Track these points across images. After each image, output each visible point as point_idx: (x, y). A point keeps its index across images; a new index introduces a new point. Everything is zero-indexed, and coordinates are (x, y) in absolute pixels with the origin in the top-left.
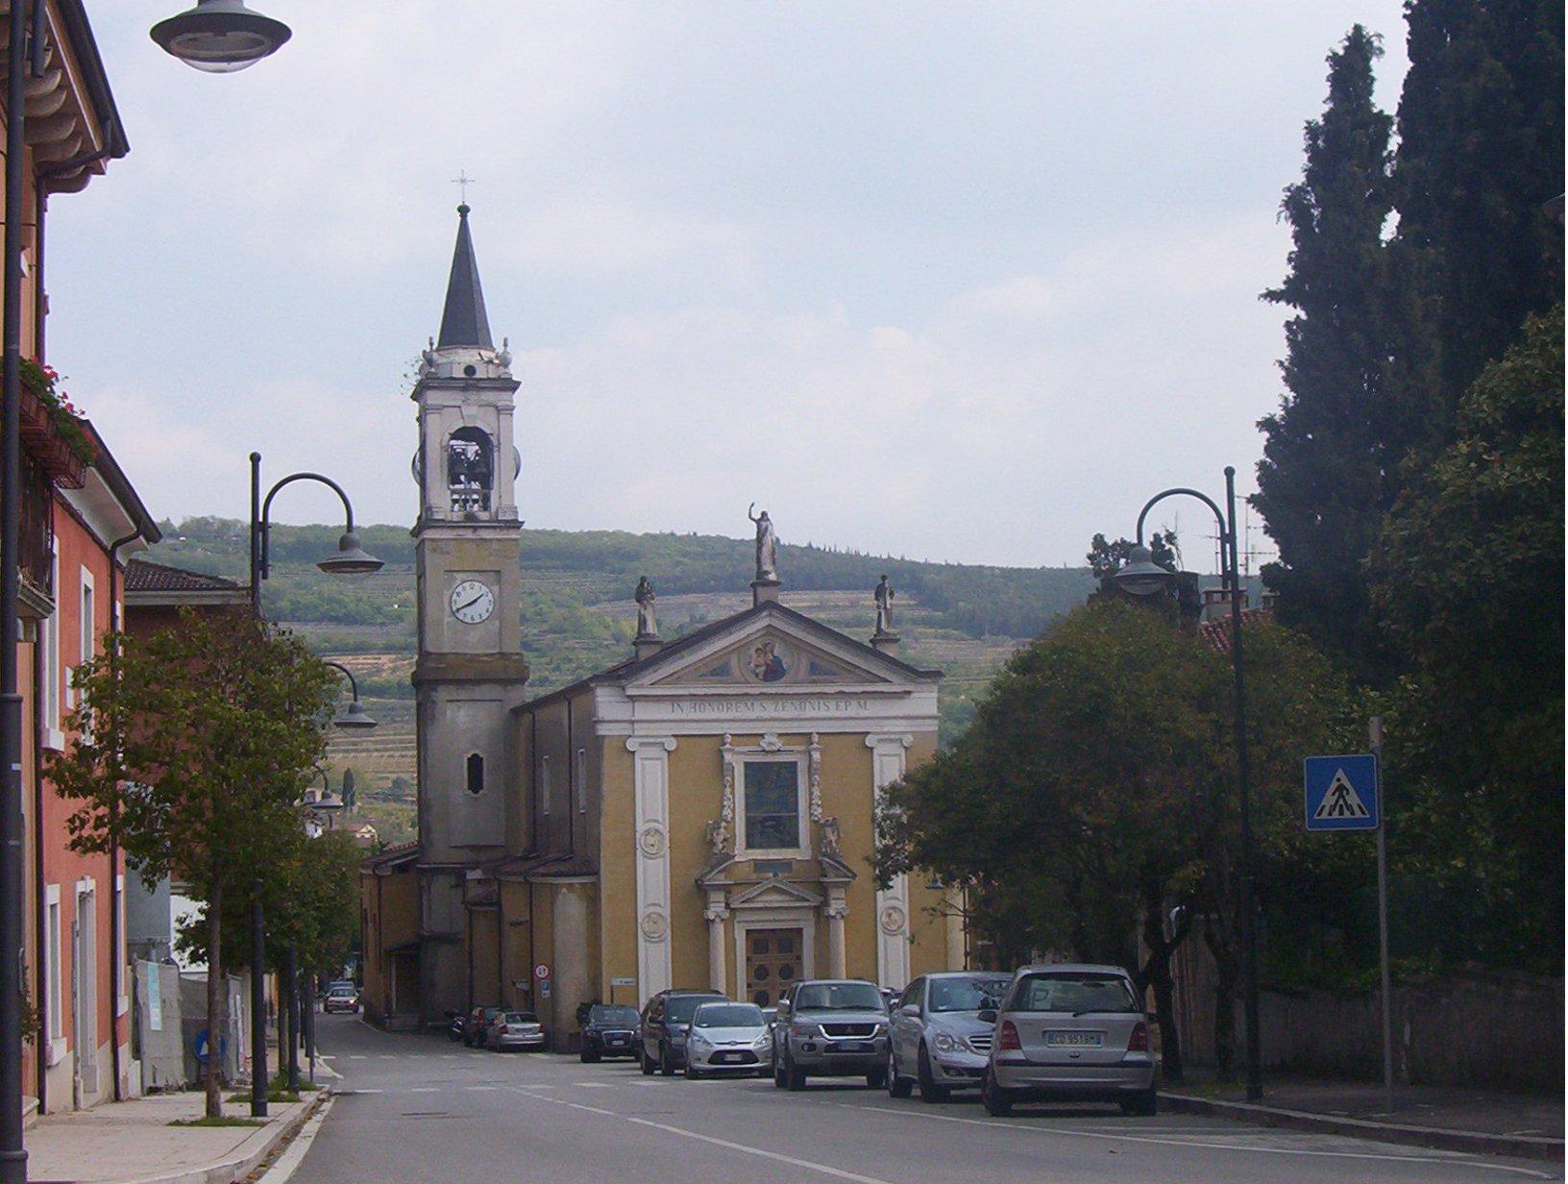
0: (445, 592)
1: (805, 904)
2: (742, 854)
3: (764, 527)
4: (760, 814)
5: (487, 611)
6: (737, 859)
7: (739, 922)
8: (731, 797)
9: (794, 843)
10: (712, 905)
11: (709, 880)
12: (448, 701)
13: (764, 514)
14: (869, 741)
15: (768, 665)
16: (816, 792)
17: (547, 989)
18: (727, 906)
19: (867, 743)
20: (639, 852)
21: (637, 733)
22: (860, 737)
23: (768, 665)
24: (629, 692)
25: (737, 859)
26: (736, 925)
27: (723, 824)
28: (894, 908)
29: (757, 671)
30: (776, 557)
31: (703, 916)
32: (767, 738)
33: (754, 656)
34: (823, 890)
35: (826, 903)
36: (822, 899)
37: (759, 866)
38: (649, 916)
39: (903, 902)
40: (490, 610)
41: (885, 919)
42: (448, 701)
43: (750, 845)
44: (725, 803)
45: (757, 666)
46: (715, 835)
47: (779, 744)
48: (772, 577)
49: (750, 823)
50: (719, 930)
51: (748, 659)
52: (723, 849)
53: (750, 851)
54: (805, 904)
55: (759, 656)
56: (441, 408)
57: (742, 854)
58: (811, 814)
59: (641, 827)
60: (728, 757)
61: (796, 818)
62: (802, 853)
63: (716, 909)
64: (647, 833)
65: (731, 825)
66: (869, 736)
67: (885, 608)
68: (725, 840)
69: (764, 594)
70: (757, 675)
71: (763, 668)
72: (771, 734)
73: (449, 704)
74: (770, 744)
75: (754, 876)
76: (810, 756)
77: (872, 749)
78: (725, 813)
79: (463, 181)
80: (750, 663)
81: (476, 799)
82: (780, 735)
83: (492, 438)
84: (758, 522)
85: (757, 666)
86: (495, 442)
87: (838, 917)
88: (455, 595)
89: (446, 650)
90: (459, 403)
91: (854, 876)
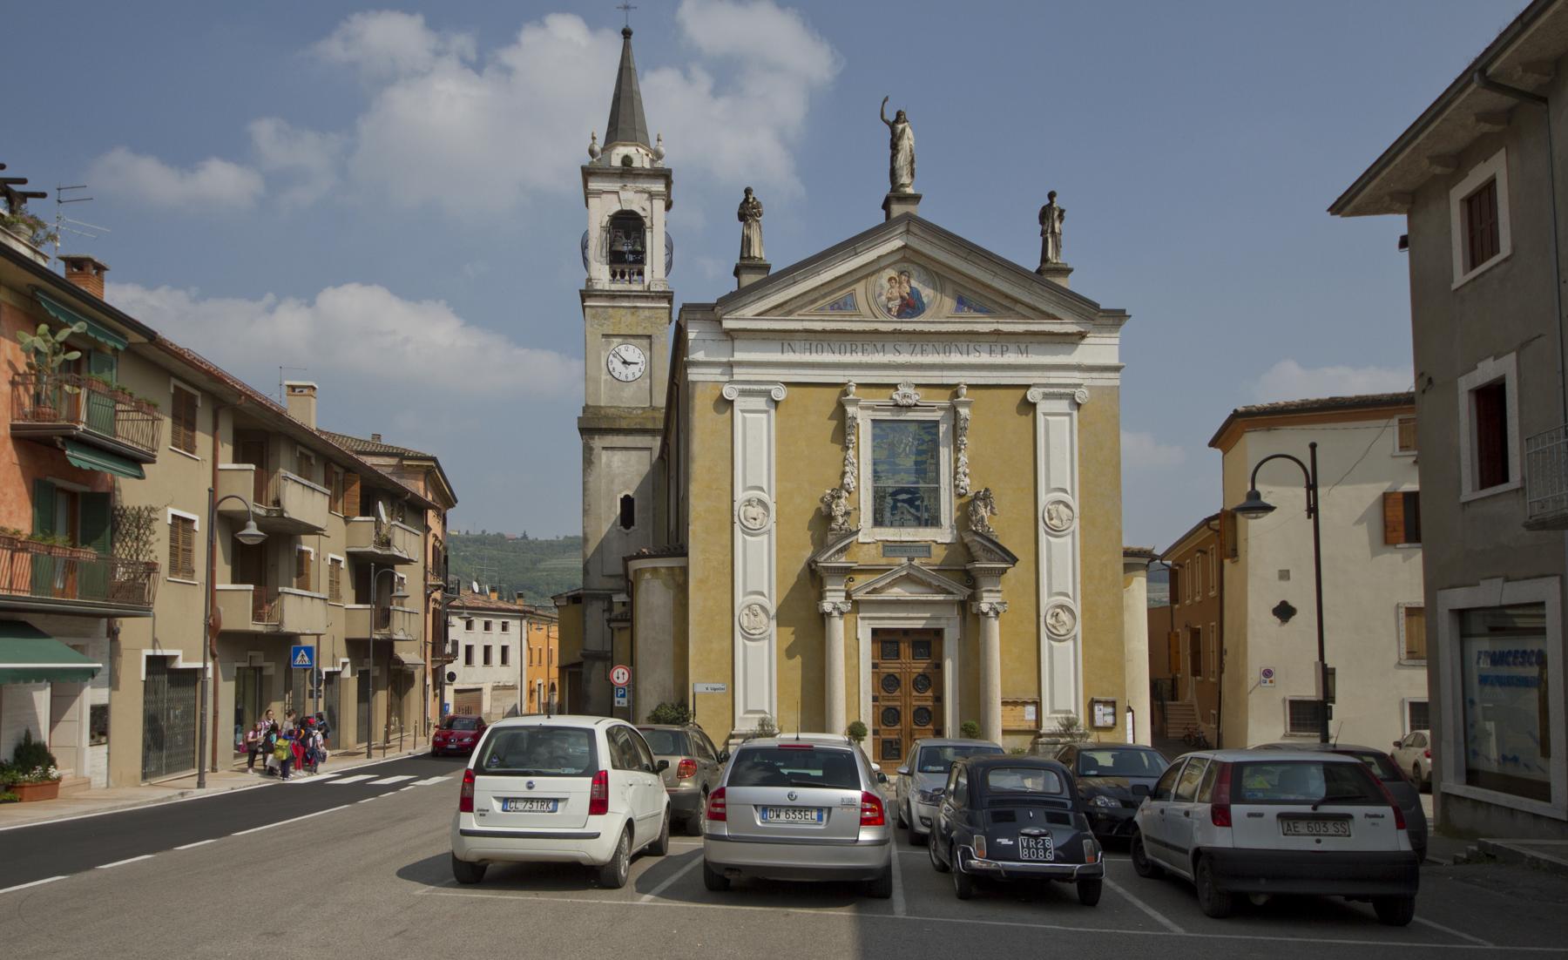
0: (603, 353)
1: (950, 597)
3: (899, 131)
4: (890, 483)
5: (640, 371)
6: (861, 538)
7: (863, 618)
8: (855, 461)
9: (934, 521)
10: (828, 594)
11: (825, 561)
12: (604, 448)
13: (899, 114)
14: (1033, 395)
15: (902, 298)
16: (963, 458)
17: (623, 696)
18: (848, 596)
19: (1029, 398)
20: (737, 527)
21: (736, 378)
22: (1021, 392)
23: (902, 298)
24: (727, 324)
25: (861, 538)
26: (859, 620)
27: (844, 494)
28: (1062, 607)
29: (890, 306)
30: (915, 166)
31: (818, 609)
32: (902, 390)
33: (886, 285)
34: (971, 581)
35: (975, 597)
36: (968, 592)
37: (890, 548)
38: (749, 607)
39: (1074, 600)
40: (642, 370)
41: (1050, 621)
42: (604, 448)
43: (878, 522)
44: (847, 469)
45: (889, 299)
46: (834, 506)
47: (915, 396)
48: (910, 190)
49: (879, 496)
50: (838, 626)
51: (877, 291)
52: (843, 524)
53: (877, 530)
54: (950, 597)
55: (892, 287)
56: (599, 193)
57: (868, 533)
58: (956, 486)
59: (740, 496)
60: (851, 410)
61: (937, 490)
62: (943, 534)
63: (834, 598)
64: (749, 502)
65: (855, 496)
66: (1032, 390)
67: (1053, 232)
68: (847, 513)
69: (897, 210)
70: (889, 310)
71: (898, 302)
72: (908, 385)
73: (604, 452)
74: (905, 396)
75: (884, 561)
76: (956, 413)
77: (1034, 405)
78: (846, 480)
79: (627, 7)
80: (880, 295)
81: (627, 534)
82: (918, 386)
83: (645, 220)
84: (892, 126)
85: (889, 299)
86: (648, 223)
87: (992, 614)
88: (611, 356)
89: (602, 404)
90: (617, 189)
91: (1014, 560)
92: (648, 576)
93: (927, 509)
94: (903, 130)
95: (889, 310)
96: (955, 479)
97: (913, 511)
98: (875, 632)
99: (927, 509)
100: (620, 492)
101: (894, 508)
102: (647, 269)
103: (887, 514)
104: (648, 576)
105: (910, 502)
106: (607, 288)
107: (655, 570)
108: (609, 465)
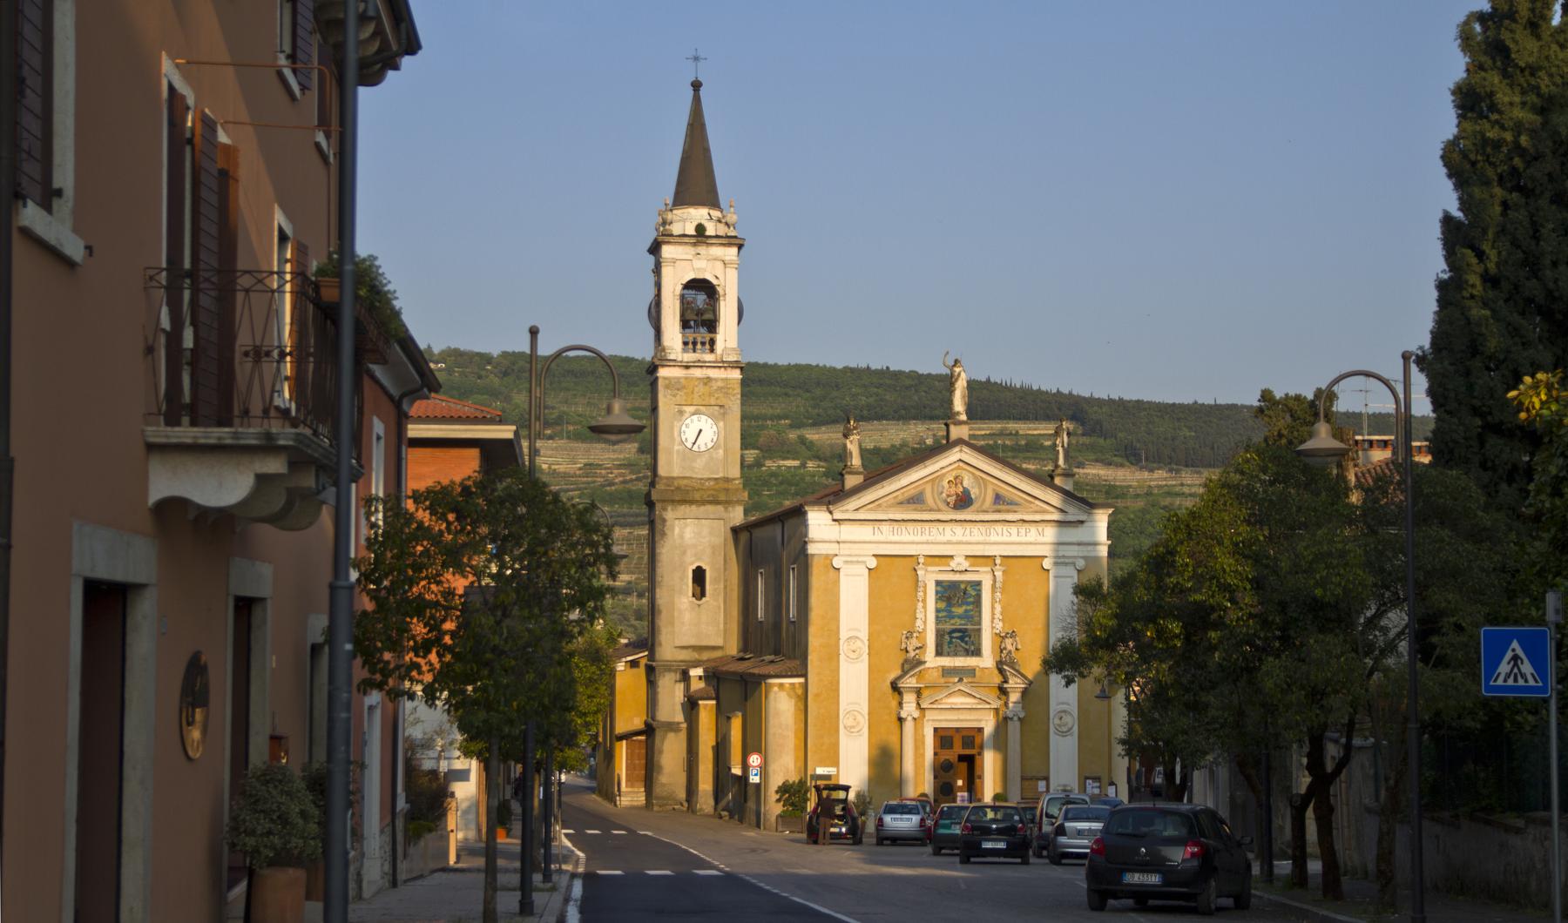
1: (988, 706)
2: (932, 660)
6: (927, 665)
13: (956, 362)
23: (957, 495)
24: (837, 516)
25: (927, 665)
28: (1065, 711)
37: (947, 672)
41: (1057, 721)
43: (939, 653)
45: (948, 496)
47: (965, 565)
49: (940, 635)
50: (909, 726)
51: (940, 489)
53: (938, 658)
54: (988, 706)
57: (932, 660)
58: (993, 628)
61: (979, 630)
63: (909, 708)
66: (1046, 560)
70: (948, 504)
71: (954, 497)
74: (959, 564)
79: (696, 59)
80: (942, 493)
81: (699, 605)
82: (967, 556)
83: (718, 288)
85: (948, 496)
86: (721, 292)
89: (675, 475)
90: (690, 257)
92: (776, 689)
93: (973, 644)
94: (959, 374)
95: (948, 504)
96: (992, 622)
97: (963, 644)
98: (936, 730)
99: (973, 644)
100: (692, 564)
101: (950, 642)
102: (719, 338)
103: (946, 647)
104: (776, 689)
105: (962, 639)
106: (680, 359)
107: (781, 685)
108: (681, 537)
